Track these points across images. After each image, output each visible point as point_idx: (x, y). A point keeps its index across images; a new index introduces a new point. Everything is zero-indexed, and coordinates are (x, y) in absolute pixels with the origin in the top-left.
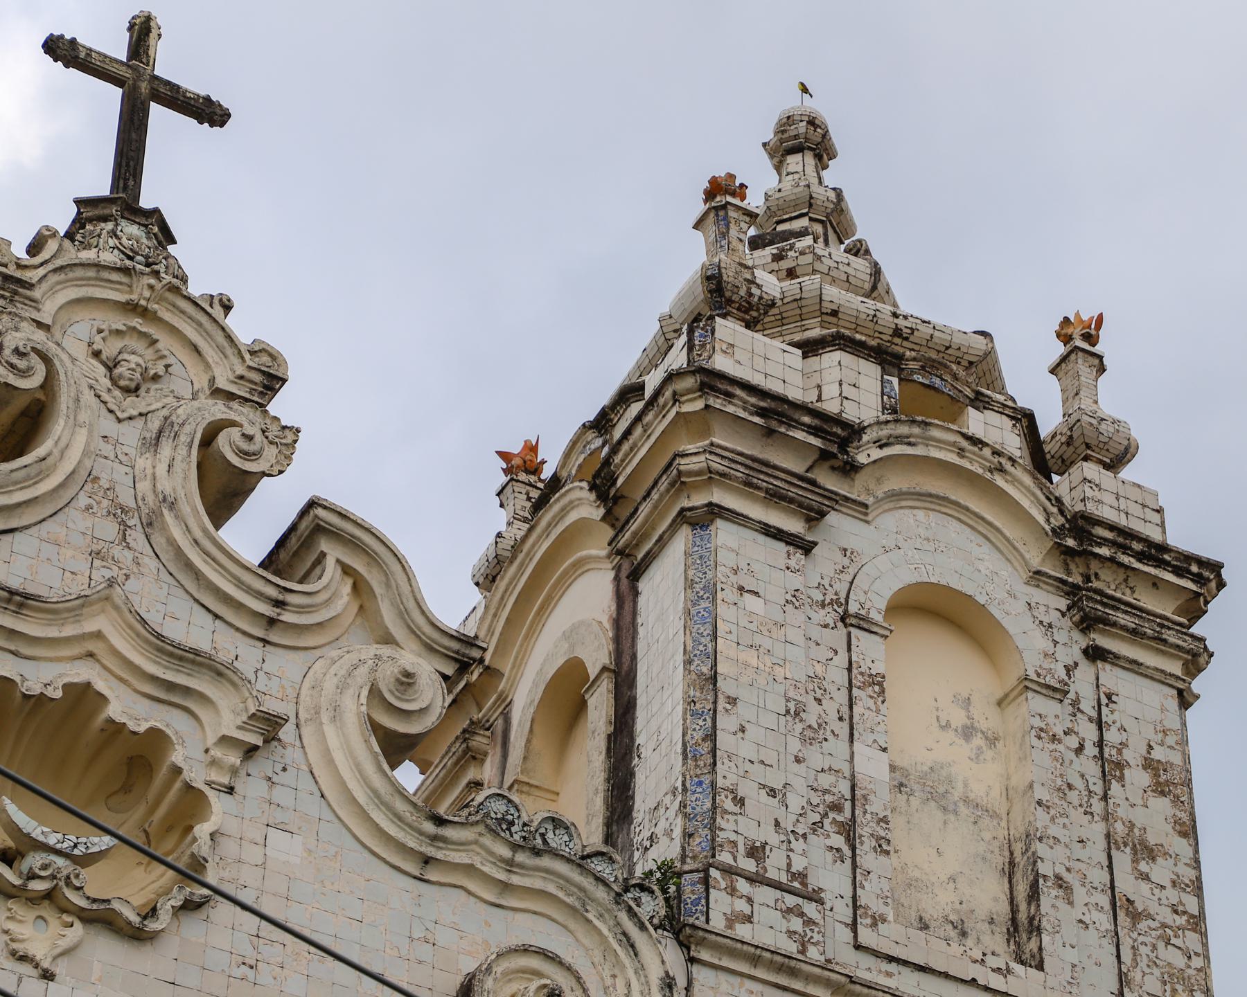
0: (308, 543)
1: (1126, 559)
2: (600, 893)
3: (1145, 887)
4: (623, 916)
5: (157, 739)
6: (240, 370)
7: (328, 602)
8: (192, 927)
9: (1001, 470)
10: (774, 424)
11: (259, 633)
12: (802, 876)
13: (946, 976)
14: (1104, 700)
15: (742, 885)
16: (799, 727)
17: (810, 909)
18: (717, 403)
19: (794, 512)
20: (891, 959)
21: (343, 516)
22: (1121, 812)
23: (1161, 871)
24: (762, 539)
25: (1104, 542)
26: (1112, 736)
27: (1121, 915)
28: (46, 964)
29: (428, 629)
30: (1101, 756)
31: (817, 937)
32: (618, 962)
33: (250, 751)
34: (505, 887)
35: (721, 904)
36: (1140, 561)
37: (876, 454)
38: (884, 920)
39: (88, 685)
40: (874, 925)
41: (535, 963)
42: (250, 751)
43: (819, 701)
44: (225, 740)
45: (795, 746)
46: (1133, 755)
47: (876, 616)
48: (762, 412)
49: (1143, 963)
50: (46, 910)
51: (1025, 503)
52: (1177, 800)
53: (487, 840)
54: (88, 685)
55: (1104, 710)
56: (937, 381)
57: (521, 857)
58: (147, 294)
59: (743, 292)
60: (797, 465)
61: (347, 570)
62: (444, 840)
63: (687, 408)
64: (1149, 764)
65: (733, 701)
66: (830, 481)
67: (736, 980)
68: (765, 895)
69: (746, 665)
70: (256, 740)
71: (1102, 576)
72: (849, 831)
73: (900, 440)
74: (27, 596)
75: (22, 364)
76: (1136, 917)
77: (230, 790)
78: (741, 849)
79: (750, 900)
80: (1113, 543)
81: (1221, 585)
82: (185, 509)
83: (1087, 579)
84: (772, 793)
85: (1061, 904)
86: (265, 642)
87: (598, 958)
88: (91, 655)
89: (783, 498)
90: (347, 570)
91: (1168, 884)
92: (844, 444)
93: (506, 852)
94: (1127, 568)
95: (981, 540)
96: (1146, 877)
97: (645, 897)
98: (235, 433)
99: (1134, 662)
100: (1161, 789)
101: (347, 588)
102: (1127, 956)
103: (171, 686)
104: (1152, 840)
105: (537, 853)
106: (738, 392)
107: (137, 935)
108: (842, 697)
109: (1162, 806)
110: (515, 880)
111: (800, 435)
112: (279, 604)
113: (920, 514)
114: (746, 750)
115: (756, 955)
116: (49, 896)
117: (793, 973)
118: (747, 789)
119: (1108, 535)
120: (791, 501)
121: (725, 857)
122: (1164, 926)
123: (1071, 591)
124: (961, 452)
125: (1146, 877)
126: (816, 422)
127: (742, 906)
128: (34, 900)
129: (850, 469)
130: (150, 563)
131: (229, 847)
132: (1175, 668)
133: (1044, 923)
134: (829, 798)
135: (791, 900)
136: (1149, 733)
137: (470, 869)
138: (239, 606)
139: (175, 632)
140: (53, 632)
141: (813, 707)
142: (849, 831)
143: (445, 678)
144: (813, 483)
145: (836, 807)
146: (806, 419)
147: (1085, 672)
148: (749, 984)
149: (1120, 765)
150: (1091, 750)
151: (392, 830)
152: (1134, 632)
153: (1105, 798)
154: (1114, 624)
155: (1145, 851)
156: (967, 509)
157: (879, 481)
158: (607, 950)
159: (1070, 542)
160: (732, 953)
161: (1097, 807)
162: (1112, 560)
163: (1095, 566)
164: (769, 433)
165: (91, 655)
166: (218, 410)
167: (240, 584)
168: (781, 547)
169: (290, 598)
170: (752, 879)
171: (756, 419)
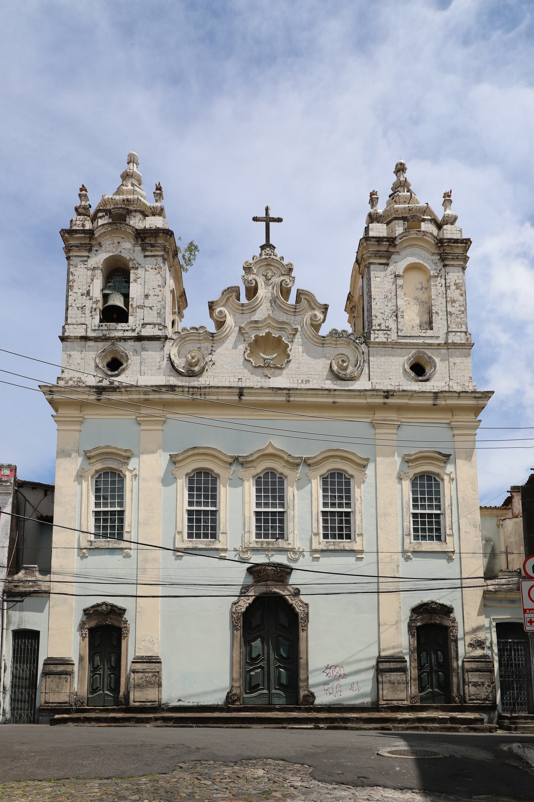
0: (299, 296)
1: (450, 244)
2: (351, 341)
3: (454, 308)
4: (355, 344)
5: (280, 338)
7: (303, 306)
9: (425, 235)
10: (379, 243)
12: (388, 327)
13: (415, 336)
14: (446, 274)
15: (376, 332)
16: (387, 300)
17: (389, 332)
18: (368, 242)
19: (385, 259)
20: (404, 336)
21: (303, 290)
22: (449, 296)
23: (456, 305)
24: (379, 266)
25: (446, 242)
26: (448, 281)
27: (448, 315)
29: (319, 305)
30: (446, 286)
31: (390, 337)
32: (356, 352)
34: (336, 344)
35: (372, 336)
36: (453, 244)
37: (400, 241)
38: (403, 330)
40: (401, 331)
41: (341, 356)
43: (391, 293)
44: (290, 334)
45: (386, 303)
46: (452, 284)
47: (401, 274)
48: (377, 241)
49: (452, 323)
51: (430, 240)
52: (461, 290)
53: (332, 338)
55: (447, 276)
56: (415, 219)
57: (337, 339)
60: (385, 249)
61: (305, 299)
62: (325, 340)
63: (364, 245)
64: (455, 284)
65: (374, 299)
66: (391, 250)
67: (376, 348)
68: (381, 332)
69: (377, 291)
70: (294, 333)
71: (447, 249)
72: (397, 316)
73: (404, 236)
74: (257, 321)
76: (451, 314)
77: (292, 342)
78: (377, 325)
79: (378, 334)
80: (448, 242)
81: (471, 242)
82: (279, 298)
83: (444, 251)
84: (382, 313)
85: (437, 317)
87: (353, 351)
89: (382, 257)
90: (305, 299)
91: (458, 306)
92: (393, 242)
93: (335, 339)
94: (451, 246)
95: (422, 250)
96: (454, 306)
97: (360, 339)
99: (453, 265)
100: (457, 288)
101: (306, 302)
102: (449, 323)
103: (281, 328)
104: (455, 299)
105: (340, 338)
106: (372, 239)
108: (395, 291)
109: (458, 291)
110: (337, 343)
111: (384, 243)
112: (295, 309)
113: (410, 249)
114: (377, 307)
115: (379, 343)
116: (268, 366)
117: (386, 344)
118: (377, 314)
119: (446, 241)
120: (384, 257)
121: (374, 328)
122: (457, 314)
123: (440, 254)
124: (417, 234)
125: (454, 306)
126: (387, 239)
127: (376, 336)
128: (266, 367)
129: (395, 246)
132: (462, 263)
133: (433, 321)
134: (393, 311)
135: (385, 332)
136: (456, 278)
137: (330, 343)
138: (290, 311)
140: (263, 325)
141: (389, 295)
142: (397, 316)
143: (323, 312)
144: (388, 252)
145: (394, 312)
146: (385, 240)
147: (443, 270)
148: (379, 348)
149: (449, 287)
150: (444, 285)
151: (317, 341)
152: (452, 259)
153: (446, 294)
154: (448, 259)
155: (454, 301)
156: (419, 245)
157: (402, 245)
158: (354, 350)
159: (439, 245)
160: (375, 344)
161: (444, 296)
162: (448, 245)
163: (445, 247)
164: (379, 244)
167: (289, 307)
168: (383, 266)
169: (297, 307)
170: (378, 330)
171: (376, 243)
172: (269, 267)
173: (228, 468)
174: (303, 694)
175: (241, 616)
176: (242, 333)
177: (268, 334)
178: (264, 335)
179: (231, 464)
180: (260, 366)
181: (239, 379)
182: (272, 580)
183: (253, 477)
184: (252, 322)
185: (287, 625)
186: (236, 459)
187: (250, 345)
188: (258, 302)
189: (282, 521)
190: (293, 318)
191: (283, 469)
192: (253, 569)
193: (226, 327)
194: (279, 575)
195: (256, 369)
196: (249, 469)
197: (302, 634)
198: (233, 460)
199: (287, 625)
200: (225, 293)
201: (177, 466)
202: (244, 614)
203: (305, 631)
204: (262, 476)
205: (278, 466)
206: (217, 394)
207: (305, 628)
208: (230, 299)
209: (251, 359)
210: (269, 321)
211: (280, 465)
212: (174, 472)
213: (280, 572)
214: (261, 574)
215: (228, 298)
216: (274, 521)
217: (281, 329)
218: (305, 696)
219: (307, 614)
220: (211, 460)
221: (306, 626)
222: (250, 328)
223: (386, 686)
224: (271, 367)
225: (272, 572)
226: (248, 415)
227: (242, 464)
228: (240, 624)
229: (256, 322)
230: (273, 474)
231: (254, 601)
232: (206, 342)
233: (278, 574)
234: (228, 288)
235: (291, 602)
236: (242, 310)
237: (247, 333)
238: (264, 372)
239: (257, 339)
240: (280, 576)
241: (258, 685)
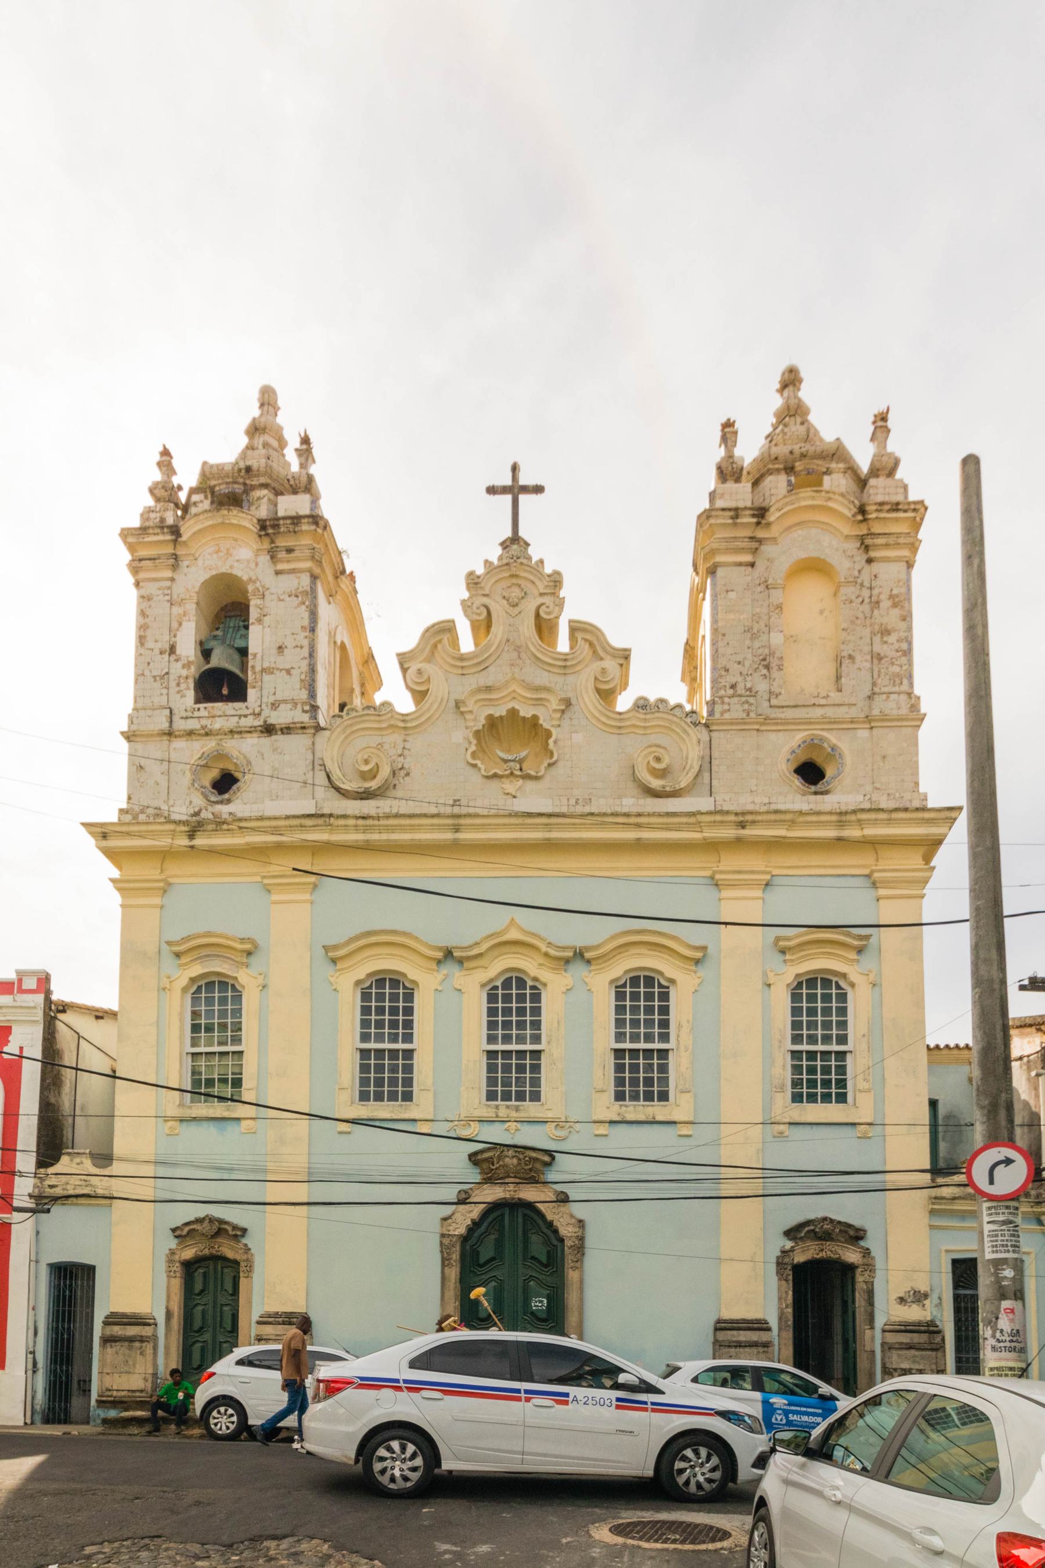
6: (546, 584)
8: (553, 771)
11: (562, 672)
28: (514, 794)
33: (563, 711)
39: (513, 708)
42: (563, 711)
50: (512, 779)
54: (513, 708)
58: (515, 569)
59: (730, 468)
75: (478, 611)
77: (559, 726)
86: (565, 674)
88: (514, 698)
98: (543, 608)
107: (537, 778)
116: (512, 774)
128: (507, 776)
130: (528, 662)
131: (560, 743)
139: (538, 682)
140: (501, 695)
165: (514, 698)
166: (540, 600)
172: (514, 581)
173: (433, 970)
176: (462, 713)
177: (513, 712)
178: (504, 713)
179: (439, 962)
180: (495, 776)
181: (455, 801)
182: (515, 1177)
183: (483, 986)
184: (479, 690)
185: (544, 1260)
186: (448, 954)
187: (477, 734)
188: (492, 650)
189: (536, 1068)
190: (560, 680)
192: (479, 1157)
193: (430, 701)
194: (527, 1167)
195: (488, 782)
196: (475, 971)
198: (442, 954)
199: (544, 1260)
200: (427, 634)
201: (339, 966)
202: (465, 1239)
205: (531, 966)
206: (412, 828)
208: (439, 647)
209: (479, 762)
210: (514, 687)
211: (534, 963)
215: (435, 646)
216: (521, 1069)
217: (539, 702)
220: (401, 956)
222: (476, 702)
224: (517, 776)
226: (472, 869)
227: (460, 961)
228: (456, 1256)
229: (488, 689)
230: (521, 983)
231: (485, 1215)
232: (393, 732)
234: (433, 626)
235: (549, 1217)
236: (462, 667)
237: (471, 712)
238: (504, 786)
239: (493, 723)
240: (531, 1170)
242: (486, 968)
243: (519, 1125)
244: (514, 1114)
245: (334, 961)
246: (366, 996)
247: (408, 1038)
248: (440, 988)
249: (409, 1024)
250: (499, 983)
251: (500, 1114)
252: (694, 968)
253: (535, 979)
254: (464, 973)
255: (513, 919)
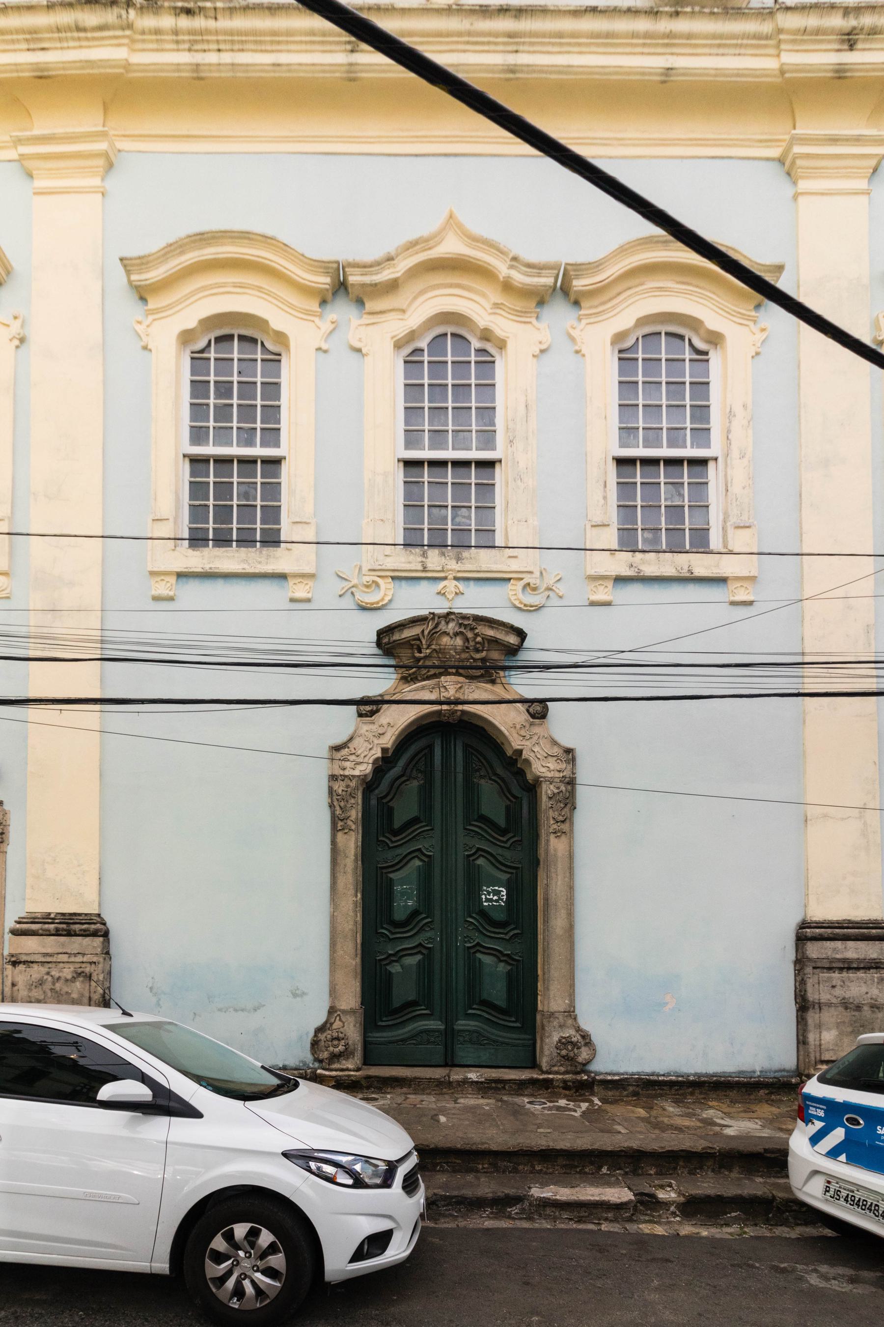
174: (556, 1038)
175: (357, 788)
191: (492, 318)
192: (396, 636)
196: (382, 318)
197: (555, 846)
202: (369, 785)
203: (563, 838)
204: (423, 344)
207: (565, 827)
212: (143, 326)
213: (482, 644)
214: (420, 652)
218: (565, 1043)
219: (571, 782)
221: (568, 820)
223: (829, 1016)
225: (459, 641)
228: (355, 814)
233: (477, 651)
241: (413, 1004)
242: (403, 311)
243: (461, 586)
244: (453, 565)
245: (142, 294)
246: (198, 360)
247: (272, 435)
248: (325, 346)
249: (272, 412)
250: (423, 344)
251: (430, 566)
252: (753, 313)
253: (486, 335)
254: (367, 319)
255: (451, 216)
